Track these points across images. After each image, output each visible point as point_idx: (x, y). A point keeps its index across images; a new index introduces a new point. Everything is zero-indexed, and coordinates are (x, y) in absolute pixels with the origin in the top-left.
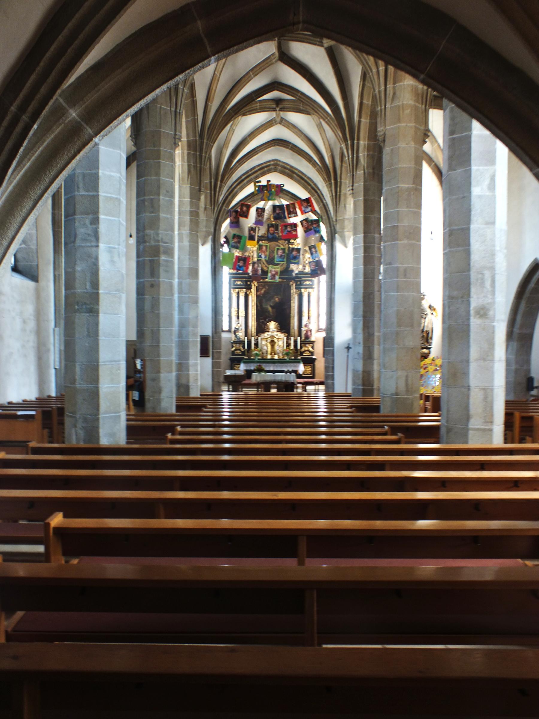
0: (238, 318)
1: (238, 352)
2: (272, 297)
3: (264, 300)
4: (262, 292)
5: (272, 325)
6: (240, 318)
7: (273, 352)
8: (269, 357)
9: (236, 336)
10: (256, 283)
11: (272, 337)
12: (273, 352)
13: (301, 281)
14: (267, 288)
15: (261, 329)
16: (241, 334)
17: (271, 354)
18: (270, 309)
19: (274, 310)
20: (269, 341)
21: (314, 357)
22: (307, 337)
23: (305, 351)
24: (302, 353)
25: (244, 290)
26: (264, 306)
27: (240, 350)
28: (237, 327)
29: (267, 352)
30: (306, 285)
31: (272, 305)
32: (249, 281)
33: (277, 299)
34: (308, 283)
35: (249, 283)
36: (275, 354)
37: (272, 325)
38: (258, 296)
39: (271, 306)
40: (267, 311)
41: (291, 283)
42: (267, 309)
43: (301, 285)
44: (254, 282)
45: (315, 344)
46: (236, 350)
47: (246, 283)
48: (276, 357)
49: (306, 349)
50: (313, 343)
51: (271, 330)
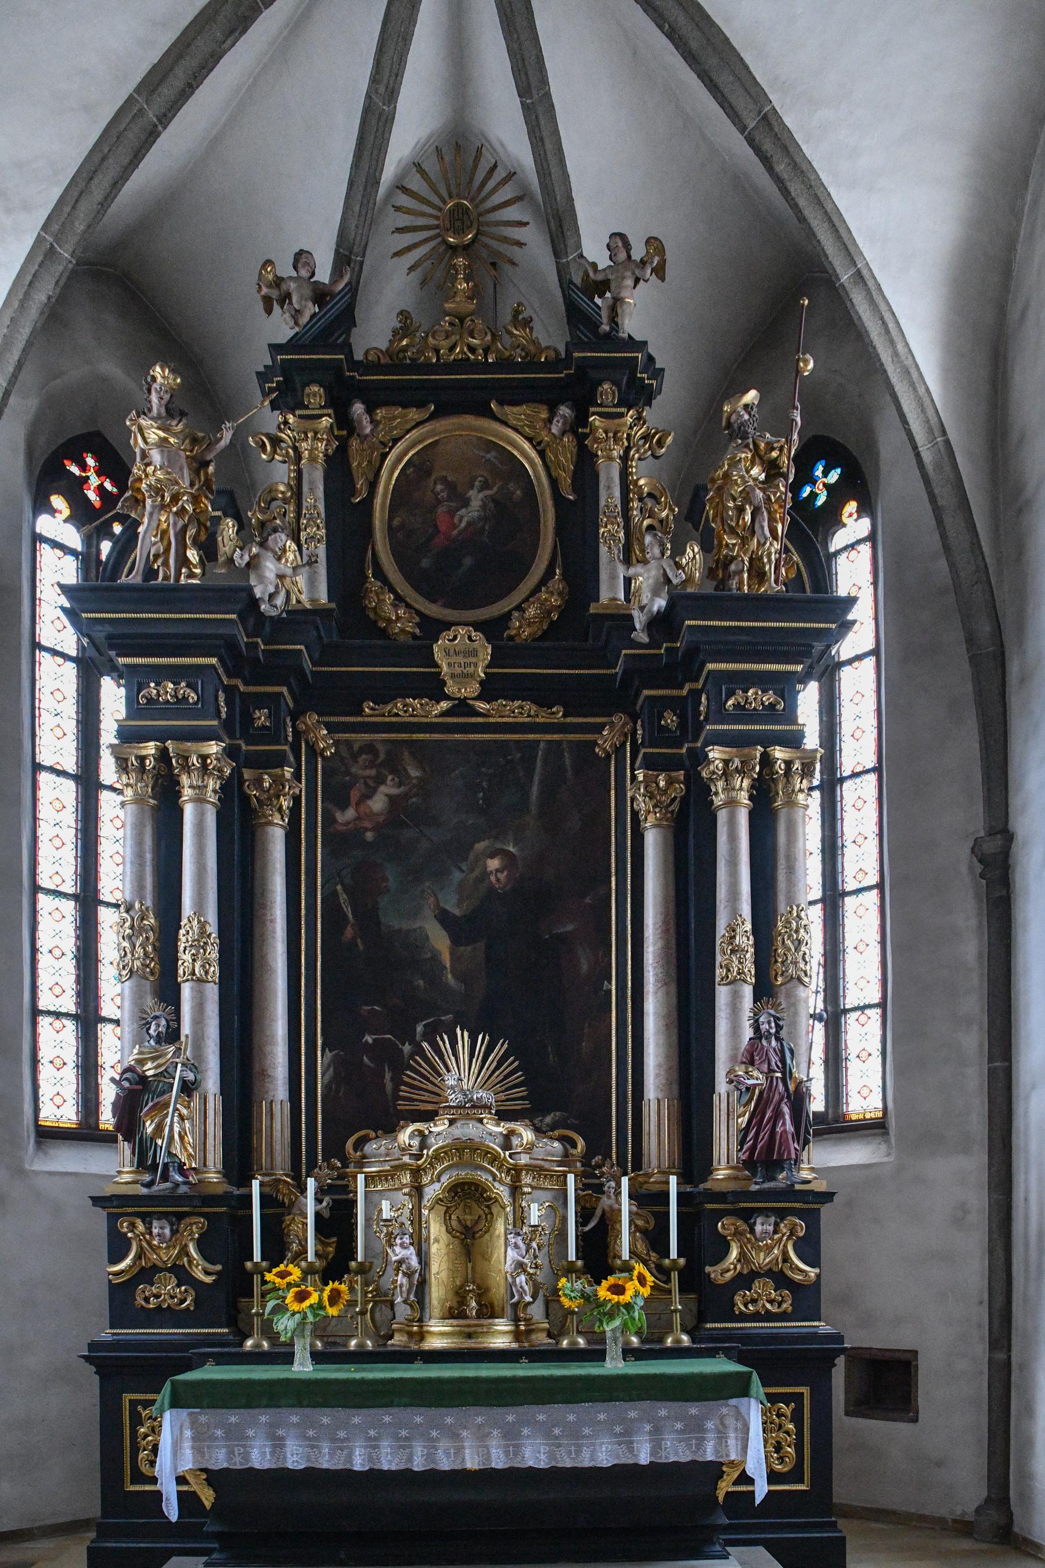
0: (167, 990)
1: (167, 1291)
2: (459, 849)
3: (391, 876)
4: (378, 803)
5: (464, 1070)
6: (186, 991)
7: (473, 1301)
8: (439, 1335)
9: (144, 1161)
10: (324, 740)
11: (463, 1151)
12: (473, 1301)
13: (685, 708)
14: (414, 773)
15: (366, 1097)
16: (191, 1135)
17: (455, 1312)
18: (440, 941)
19: (474, 951)
20: (432, 1191)
21: (823, 1327)
22: (765, 1157)
23: (745, 1280)
24: (709, 1302)
25: (213, 748)
26: (393, 921)
27: (182, 1275)
28: (150, 1069)
29: (421, 1287)
30: (742, 714)
31: (453, 906)
32: (261, 701)
33: (494, 864)
34: (756, 697)
35: (262, 717)
36: (489, 1311)
37: (464, 1070)
38: (339, 842)
39: (444, 918)
40: (411, 954)
41: (606, 740)
42: (417, 943)
43: (691, 727)
44: (311, 719)
45: (826, 1211)
46: (146, 1274)
47: (248, 719)
48: (500, 1336)
49: (762, 1260)
50: (809, 1204)
51: (454, 1098)
